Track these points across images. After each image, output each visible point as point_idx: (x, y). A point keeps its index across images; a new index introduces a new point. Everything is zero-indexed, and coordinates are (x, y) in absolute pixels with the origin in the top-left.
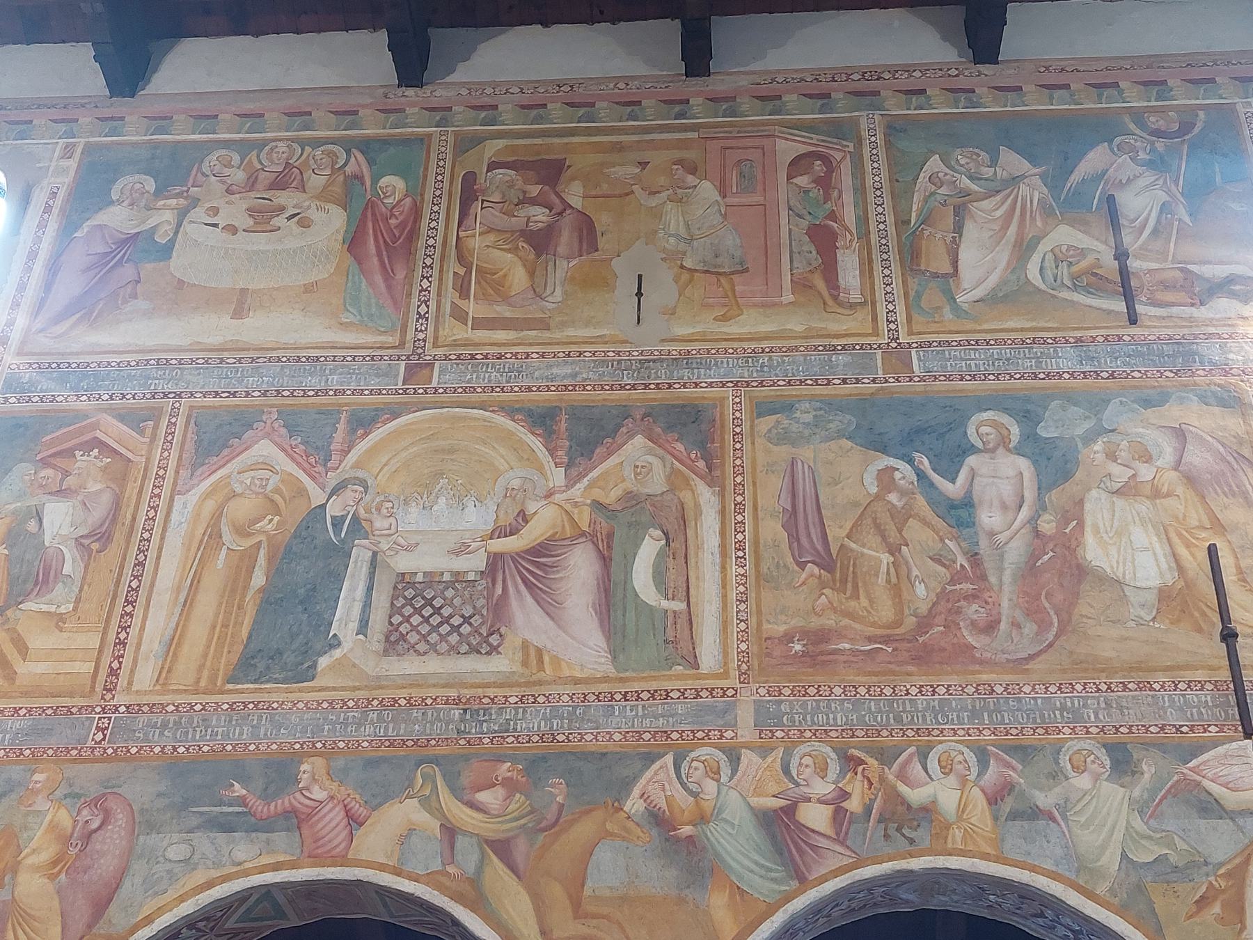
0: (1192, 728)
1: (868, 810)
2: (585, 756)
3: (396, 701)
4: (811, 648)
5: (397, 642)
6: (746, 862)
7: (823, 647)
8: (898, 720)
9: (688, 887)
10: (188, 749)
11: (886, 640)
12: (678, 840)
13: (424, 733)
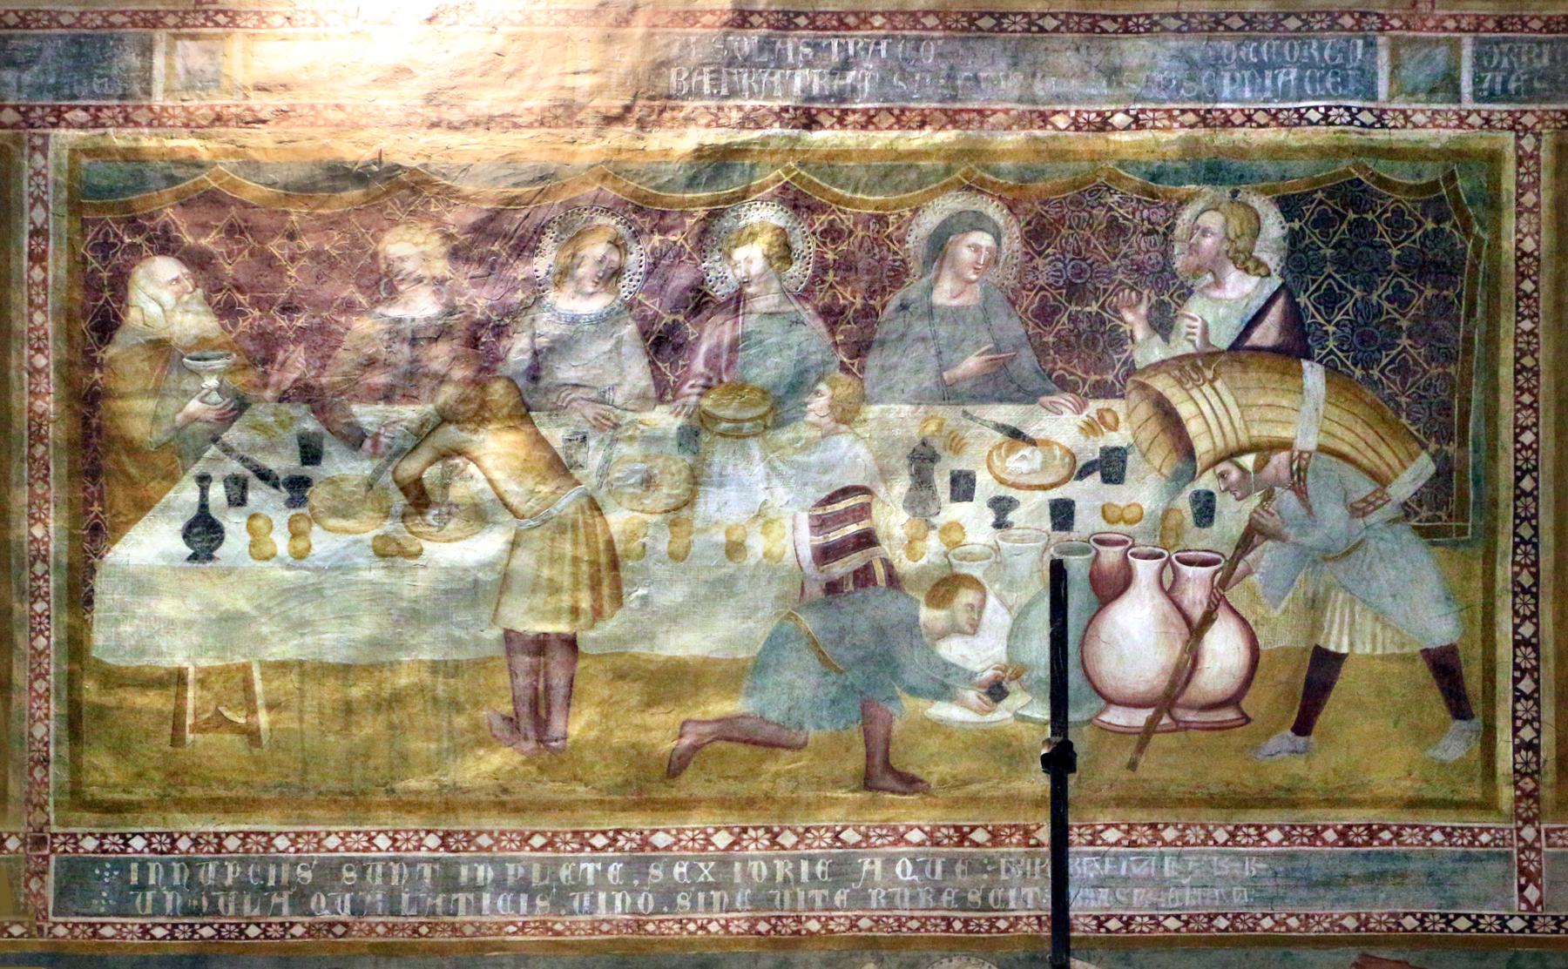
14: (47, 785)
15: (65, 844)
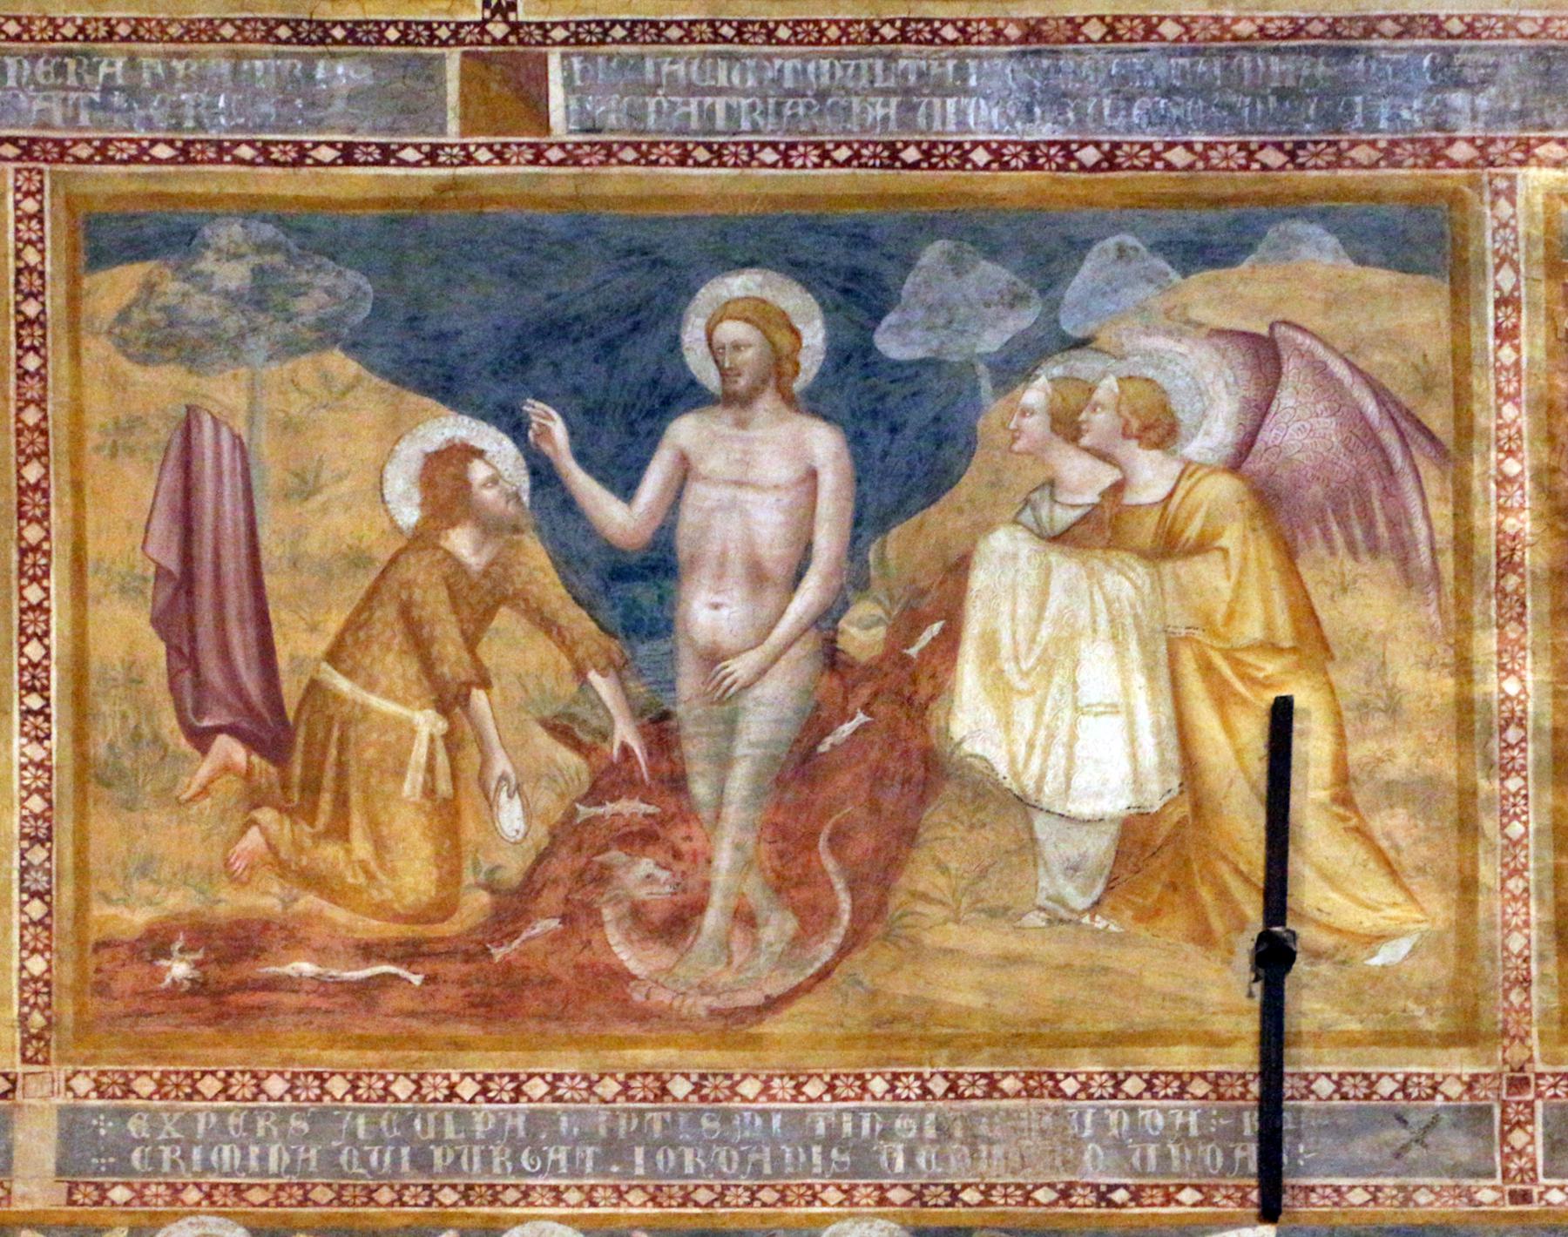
0: (1136, 1195)
4: (214, 971)
7: (245, 970)
8: (422, 1161)
11: (410, 953)
14: (1529, 1012)
15: (1555, 1086)
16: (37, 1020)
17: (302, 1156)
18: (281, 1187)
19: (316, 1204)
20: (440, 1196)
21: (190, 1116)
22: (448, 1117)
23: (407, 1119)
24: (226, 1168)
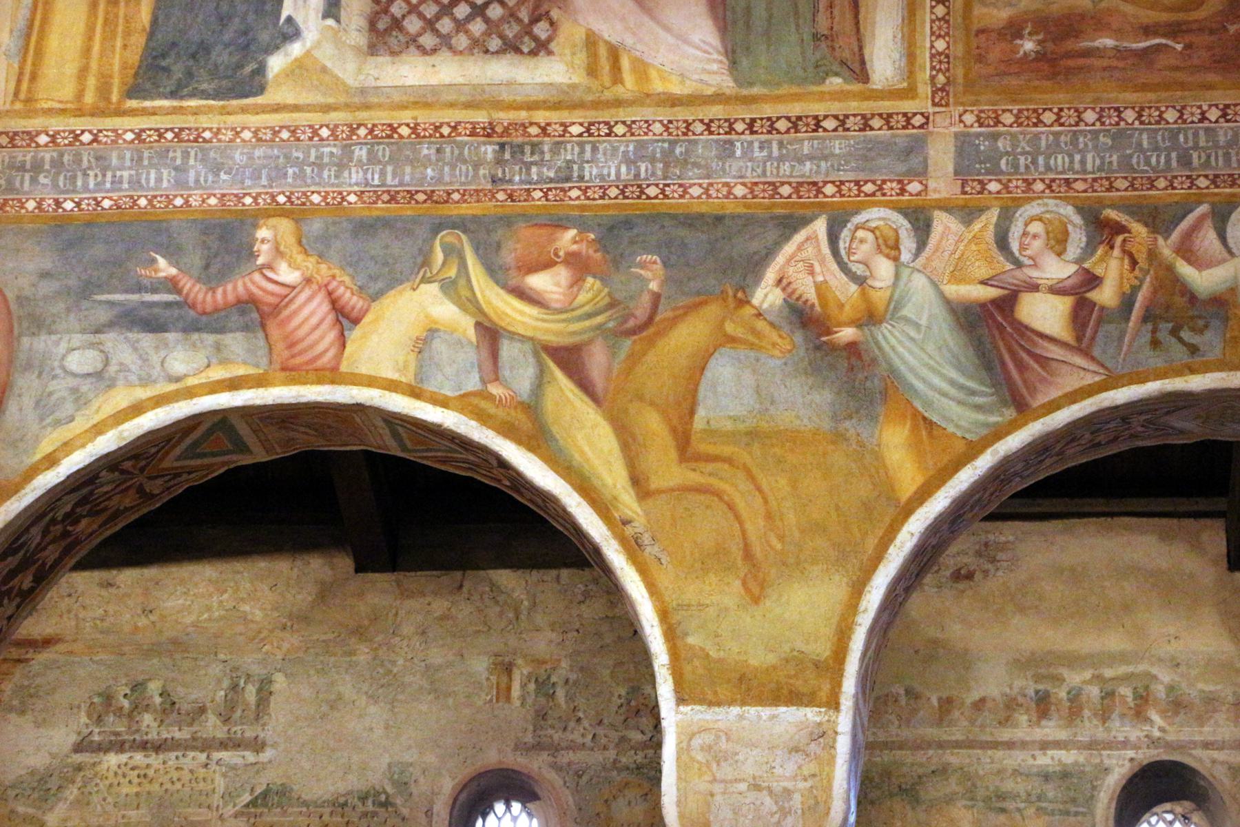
1: (1127, 303)
2: (691, 221)
3: (394, 130)
4: (1050, 46)
5: (387, 31)
6: (936, 381)
7: (1070, 45)
8: (1185, 161)
9: (850, 417)
10: (78, 204)
11: (1174, 30)
12: (833, 348)
13: (440, 180)
16: (941, 79)
17: (1107, 160)
18: (1095, 180)
19: (1118, 190)
20: (1196, 182)
21: (1037, 136)
22: (1201, 133)
23: (1174, 135)
24: (1060, 168)
